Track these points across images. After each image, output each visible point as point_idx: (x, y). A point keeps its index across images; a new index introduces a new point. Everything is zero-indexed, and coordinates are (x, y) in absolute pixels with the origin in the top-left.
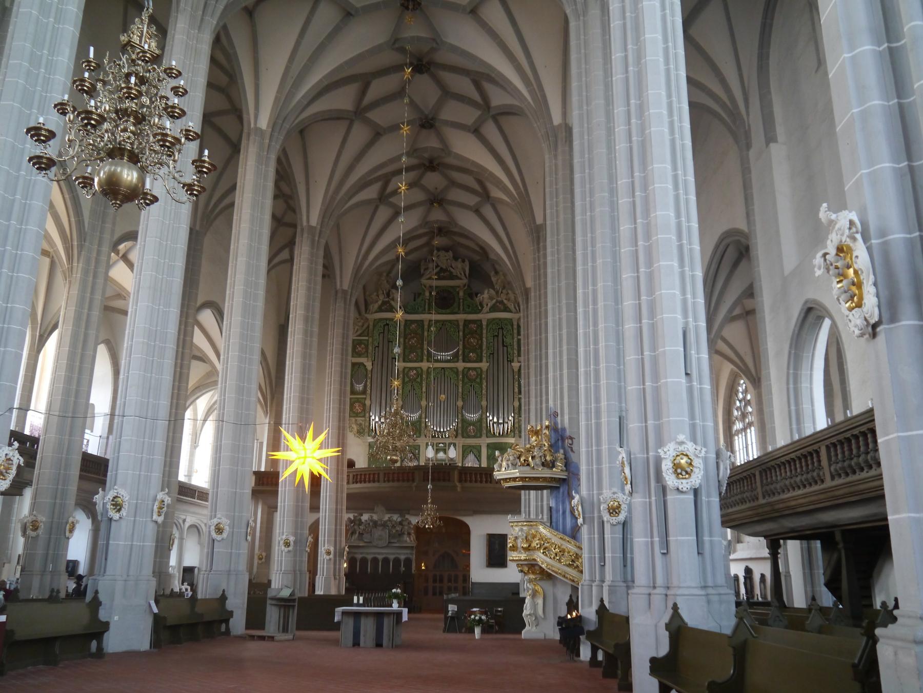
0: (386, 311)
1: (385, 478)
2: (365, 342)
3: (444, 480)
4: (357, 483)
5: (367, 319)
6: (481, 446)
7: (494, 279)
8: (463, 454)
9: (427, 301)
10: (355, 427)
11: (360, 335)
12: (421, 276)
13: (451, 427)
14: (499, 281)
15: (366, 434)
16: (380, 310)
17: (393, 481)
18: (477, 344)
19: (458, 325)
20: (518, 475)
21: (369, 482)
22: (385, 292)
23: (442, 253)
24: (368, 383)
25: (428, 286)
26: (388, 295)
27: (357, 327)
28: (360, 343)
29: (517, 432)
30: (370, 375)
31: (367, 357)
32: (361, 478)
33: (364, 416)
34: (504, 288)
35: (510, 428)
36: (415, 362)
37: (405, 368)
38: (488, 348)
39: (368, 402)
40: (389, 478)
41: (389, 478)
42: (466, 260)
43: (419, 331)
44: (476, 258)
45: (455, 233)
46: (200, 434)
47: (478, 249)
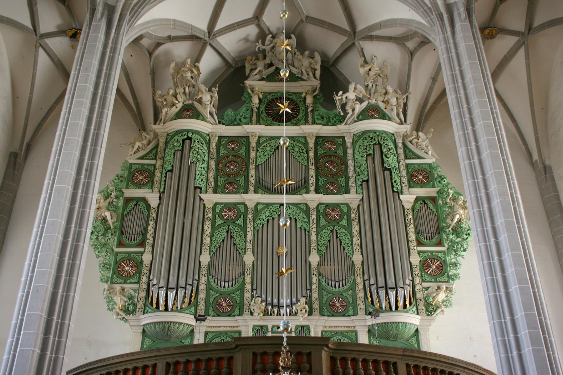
0: (188, 117)
2: (149, 167)
5: (156, 135)
9: (255, 110)
10: (119, 301)
11: (142, 158)
12: (247, 78)
15: (139, 312)
16: (179, 115)
19: (306, 144)
27: (138, 144)
28: (142, 170)
29: (422, 306)
30: (154, 215)
31: (152, 188)
33: (138, 282)
37: (216, 204)
38: (357, 174)
39: (147, 258)
43: (242, 152)
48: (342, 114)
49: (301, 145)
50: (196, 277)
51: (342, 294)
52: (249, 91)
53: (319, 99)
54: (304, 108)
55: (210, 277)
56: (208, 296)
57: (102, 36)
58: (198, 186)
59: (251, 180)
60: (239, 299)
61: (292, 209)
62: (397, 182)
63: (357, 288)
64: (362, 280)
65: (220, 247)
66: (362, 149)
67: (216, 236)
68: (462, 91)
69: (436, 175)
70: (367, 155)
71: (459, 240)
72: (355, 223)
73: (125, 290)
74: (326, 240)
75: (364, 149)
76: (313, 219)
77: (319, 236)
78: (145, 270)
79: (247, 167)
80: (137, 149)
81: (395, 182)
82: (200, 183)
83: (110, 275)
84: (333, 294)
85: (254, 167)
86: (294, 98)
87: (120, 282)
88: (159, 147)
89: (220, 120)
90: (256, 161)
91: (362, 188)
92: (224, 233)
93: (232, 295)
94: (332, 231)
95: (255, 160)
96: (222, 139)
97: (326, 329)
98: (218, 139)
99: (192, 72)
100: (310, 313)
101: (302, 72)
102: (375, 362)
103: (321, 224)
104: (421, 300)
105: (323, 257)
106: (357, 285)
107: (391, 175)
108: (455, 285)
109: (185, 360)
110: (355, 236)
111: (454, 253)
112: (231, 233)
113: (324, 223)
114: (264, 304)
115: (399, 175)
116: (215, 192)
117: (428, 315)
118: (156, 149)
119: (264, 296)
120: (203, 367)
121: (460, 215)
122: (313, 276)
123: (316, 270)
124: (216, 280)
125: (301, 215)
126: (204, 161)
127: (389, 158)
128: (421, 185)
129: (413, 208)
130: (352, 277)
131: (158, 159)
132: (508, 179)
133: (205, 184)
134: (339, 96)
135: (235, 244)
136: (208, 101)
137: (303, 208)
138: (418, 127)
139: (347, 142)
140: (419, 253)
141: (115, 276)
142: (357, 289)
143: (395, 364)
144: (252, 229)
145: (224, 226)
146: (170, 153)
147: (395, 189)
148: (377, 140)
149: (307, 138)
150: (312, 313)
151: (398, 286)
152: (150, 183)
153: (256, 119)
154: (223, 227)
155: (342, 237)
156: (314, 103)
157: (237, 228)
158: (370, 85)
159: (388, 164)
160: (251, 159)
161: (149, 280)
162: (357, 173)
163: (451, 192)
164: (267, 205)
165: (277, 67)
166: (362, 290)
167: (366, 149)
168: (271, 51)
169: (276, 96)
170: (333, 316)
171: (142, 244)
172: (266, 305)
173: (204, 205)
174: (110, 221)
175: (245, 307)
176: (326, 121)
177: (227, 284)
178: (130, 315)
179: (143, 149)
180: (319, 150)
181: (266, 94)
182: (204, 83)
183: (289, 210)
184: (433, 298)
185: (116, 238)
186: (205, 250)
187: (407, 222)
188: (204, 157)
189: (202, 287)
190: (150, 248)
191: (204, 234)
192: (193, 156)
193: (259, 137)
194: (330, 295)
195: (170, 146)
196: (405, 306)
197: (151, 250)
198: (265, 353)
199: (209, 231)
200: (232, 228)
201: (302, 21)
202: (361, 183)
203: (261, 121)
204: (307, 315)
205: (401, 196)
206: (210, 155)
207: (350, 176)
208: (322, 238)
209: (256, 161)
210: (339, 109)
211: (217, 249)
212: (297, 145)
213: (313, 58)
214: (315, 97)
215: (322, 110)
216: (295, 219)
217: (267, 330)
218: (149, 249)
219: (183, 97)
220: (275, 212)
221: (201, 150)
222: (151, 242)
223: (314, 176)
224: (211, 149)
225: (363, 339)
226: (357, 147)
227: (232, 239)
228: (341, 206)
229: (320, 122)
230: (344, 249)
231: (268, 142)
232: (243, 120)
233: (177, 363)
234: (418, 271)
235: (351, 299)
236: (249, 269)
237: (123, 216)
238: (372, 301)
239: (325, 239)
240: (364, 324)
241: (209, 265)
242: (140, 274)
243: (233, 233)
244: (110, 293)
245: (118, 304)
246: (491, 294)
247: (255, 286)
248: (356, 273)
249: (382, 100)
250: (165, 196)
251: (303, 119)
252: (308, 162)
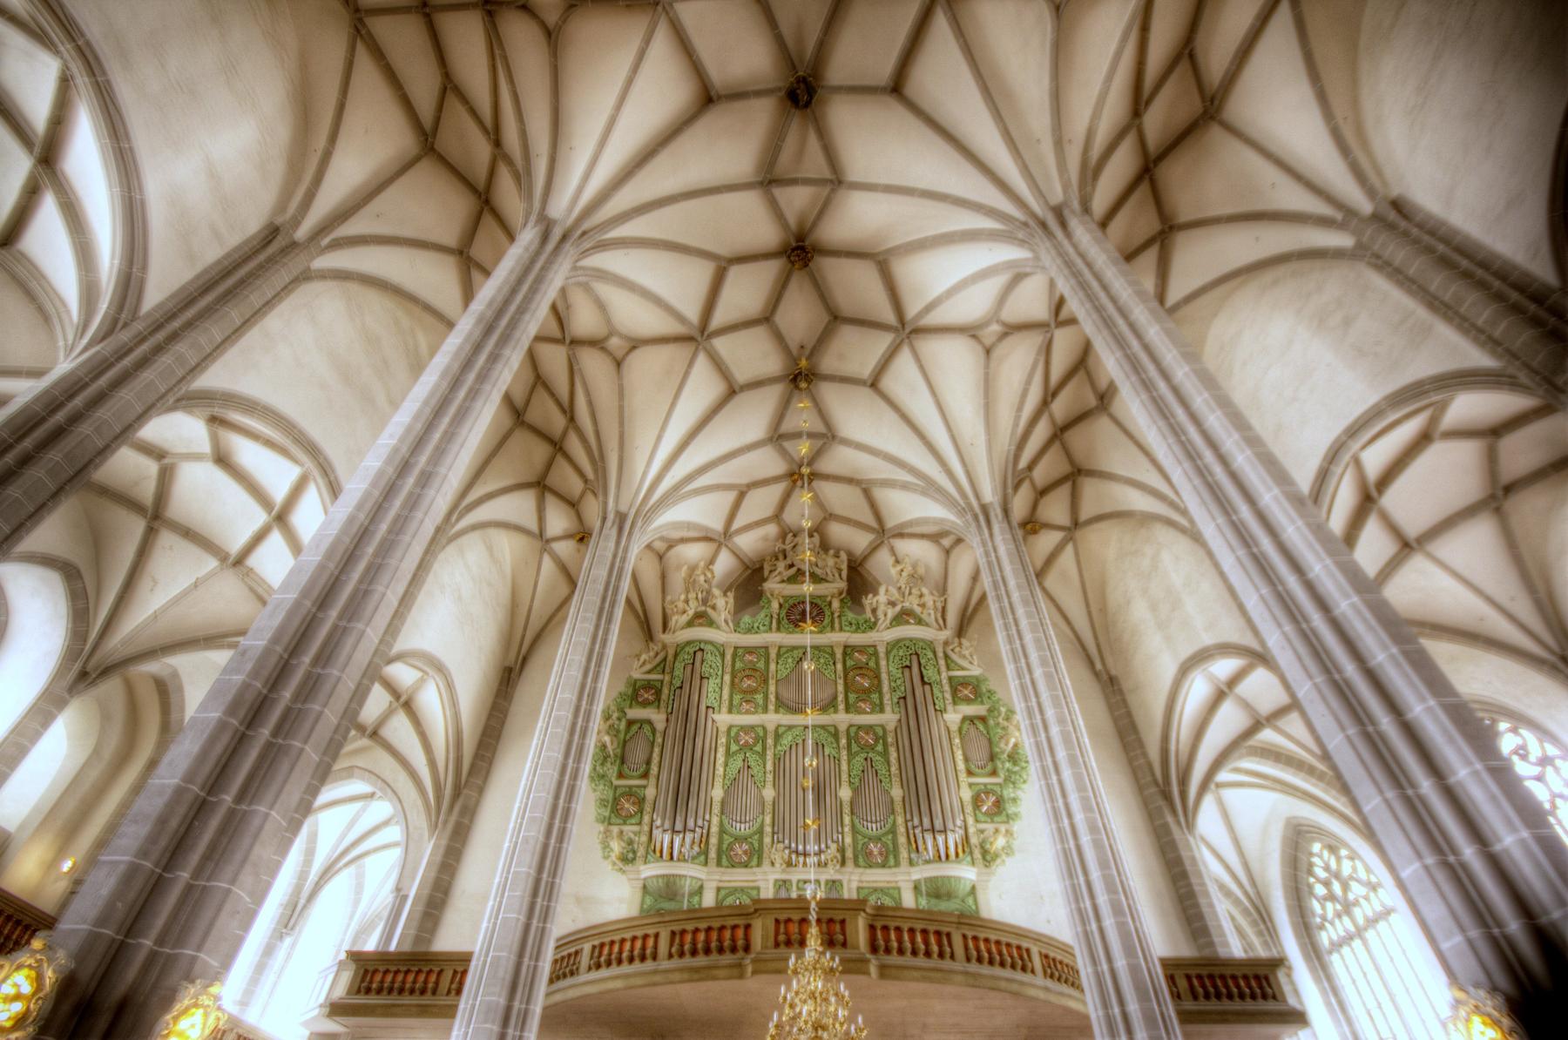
0: (701, 625)
1: (671, 945)
4: (598, 966)
5: (664, 647)
6: (899, 889)
10: (616, 847)
11: (649, 672)
12: (764, 580)
13: (829, 842)
15: (639, 861)
18: (872, 685)
19: (833, 655)
22: (700, 596)
25: (776, 592)
26: (705, 602)
27: (644, 657)
28: (648, 686)
29: (977, 854)
31: (658, 707)
33: (640, 824)
39: (650, 792)
40: (682, 945)
41: (682, 945)
43: (761, 665)
46: (305, 907)
48: (873, 620)
50: (707, 817)
52: (769, 595)
55: (724, 817)
56: (721, 841)
57: (612, 545)
68: (1006, 600)
69: (984, 690)
71: (1017, 769)
78: (648, 808)
79: (766, 681)
83: (607, 814)
85: (774, 681)
86: (819, 602)
94: (866, 759)
99: (705, 575)
100: (843, 863)
102: (924, 932)
105: (856, 791)
107: (932, 690)
108: (1016, 827)
111: (1011, 786)
114: (787, 851)
116: (730, 711)
117: (986, 866)
119: (787, 842)
121: (1016, 737)
128: (968, 701)
129: (960, 730)
130: (892, 817)
132: (1067, 703)
138: (961, 631)
140: (970, 785)
143: (948, 935)
147: (937, 707)
156: (842, 607)
158: (903, 586)
161: (652, 821)
163: (1003, 710)
164: (790, 728)
170: (871, 867)
171: (645, 775)
172: (790, 853)
174: (610, 748)
181: (787, 598)
182: (718, 587)
184: (991, 843)
185: (616, 769)
187: (954, 748)
189: (714, 829)
192: (706, 668)
193: (780, 647)
194: (866, 840)
195: (680, 658)
196: (957, 855)
198: (789, 920)
201: (825, 519)
203: (782, 628)
205: (945, 715)
210: (869, 614)
213: (838, 557)
214: (842, 601)
215: (850, 616)
219: (696, 603)
225: (908, 900)
226: (891, 658)
229: (848, 628)
232: (761, 628)
233: (683, 932)
237: (625, 742)
238: (917, 848)
240: (907, 878)
241: (723, 803)
242: (642, 813)
246: (1059, 847)
247: (776, 828)
250: (673, 718)
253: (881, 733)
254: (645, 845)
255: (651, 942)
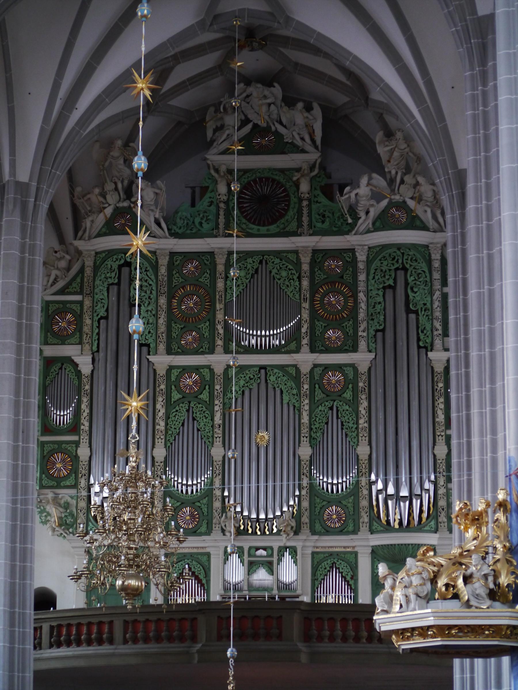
1: (125, 633)
2: (73, 306)
3: (268, 637)
4: (59, 645)
5: (79, 253)
6: (356, 554)
7: (382, 150)
8: (314, 574)
9: (222, 205)
11: (62, 292)
12: (209, 144)
13: (285, 509)
14: (396, 154)
17: (146, 640)
18: (345, 307)
19: (298, 264)
20: (431, 621)
21: (89, 643)
22: (120, 186)
23: (256, 90)
24: (84, 406)
25: (223, 169)
27: (54, 273)
30: (87, 387)
31: (80, 343)
32: (69, 634)
33: (75, 486)
34: (408, 170)
35: (425, 508)
36: (196, 352)
37: (171, 368)
38: (370, 317)
39: (83, 452)
40: (135, 632)
41: (135, 632)
42: (315, 105)
43: (205, 279)
44: (341, 99)
45: (287, 41)
47: (341, 77)
48: (350, 221)
49: (290, 267)
51: (340, 502)
53: (319, 182)
54: (296, 200)
58: (144, 342)
59: (218, 328)
60: (206, 510)
61: (277, 374)
62: (425, 332)
63: (360, 493)
64: (368, 483)
65: (178, 434)
66: (379, 276)
67: (173, 418)
70: (384, 288)
72: (363, 397)
73: (60, 496)
74: (322, 422)
75: (381, 278)
76: (304, 390)
77: (313, 416)
80: (55, 279)
81: (422, 332)
82: (147, 338)
84: (329, 502)
85: (222, 306)
87: (51, 484)
88: (86, 275)
89: (170, 227)
90: (226, 295)
91: (376, 341)
92: (184, 414)
93: (198, 504)
95: (223, 294)
96: (175, 258)
97: (318, 550)
98: (169, 259)
101: (293, 136)
103: (316, 399)
104: (443, 509)
106: (360, 490)
107: (417, 320)
109: (144, 620)
110: (362, 416)
112: (193, 412)
113: (320, 397)
115: (431, 317)
116: (169, 352)
118: (80, 275)
120: (165, 628)
122: (302, 477)
123: (307, 469)
124: (176, 483)
125: (289, 384)
126: (151, 299)
127: (416, 293)
131: (85, 295)
133: (154, 335)
134: (346, 194)
135: (198, 430)
136: (151, 201)
137: (291, 372)
139: (358, 260)
141: (44, 476)
142: (360, 495)
144: (222, 407)
145: (183, 403)
146: (101, 288)
147: (421, 344)
148: (400, 261)
149: (300, 255)
150: (300, 528)
151: (413, 494)
152: (78, 333)
153: (224, 220)
154: (181, 405)
155: (344, 417)
156: (312, 188)
157: (200, 405)
158: (393, 172)
159: (413, 304)
160: (217, 293)
162: (370, 314)
165: (256, 122)
166: (367, 496)
167: (384, 276)
168: (244, 101)
169: (253, 178)
173: (155, 370)
175: (214, 521)
176: (328, 224)
177: (189, 489)
178: (68, 530)
179: (62, 278)
180: (317, 274)
183: (272, 376)
186: (160, 440)
188: (151, 292)
190: (86, 438)
191: (157, 417)
197: (88, 441)
199: (163, 411)
200: (195, 405)
202: (374, 333)
204: (292, 534)
205: (430, 354)
206: (159, 288)
207: (360, 319)
208: (317, 420)
209: (226, 295)
211: (175, 437)
212: (285, 266)
214: (312, 179)
216: (281, 389)
217: (243, 553)
218: (84, 439)
219: (116, 197)
220: (252, 379)
221: (146, 281)
222: (87, 428)
223: (308, 321)
224: (160, 277)
226: (372, 271)
227: (195, 422)
228: (345, 368)
229: (319, 225)
230: (346, 435)
231: (242, 263)
232: (205, 225)
233: (135, 621)
234: (444, 467)
235: (352, 509)
236: (218, 468)
239: (320, 421)
243: (196, 413)
244: (41, 502)
245: (52, 515)
248: (361, 472)
249: (411, 196)
251: (294, 218)
252: (300, 295)
253: (351, 376)
254: (84, 511)
255: (106, 629)
